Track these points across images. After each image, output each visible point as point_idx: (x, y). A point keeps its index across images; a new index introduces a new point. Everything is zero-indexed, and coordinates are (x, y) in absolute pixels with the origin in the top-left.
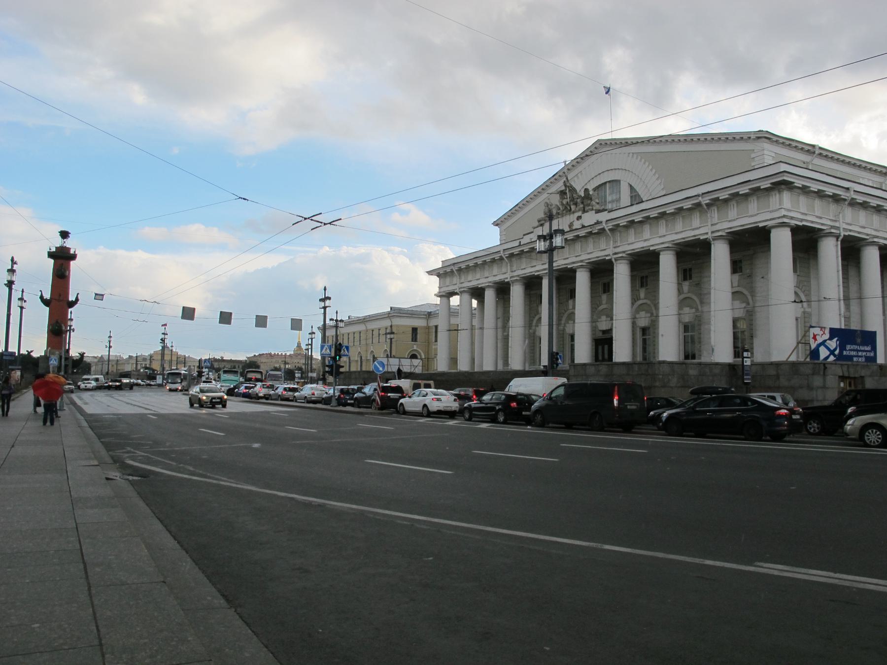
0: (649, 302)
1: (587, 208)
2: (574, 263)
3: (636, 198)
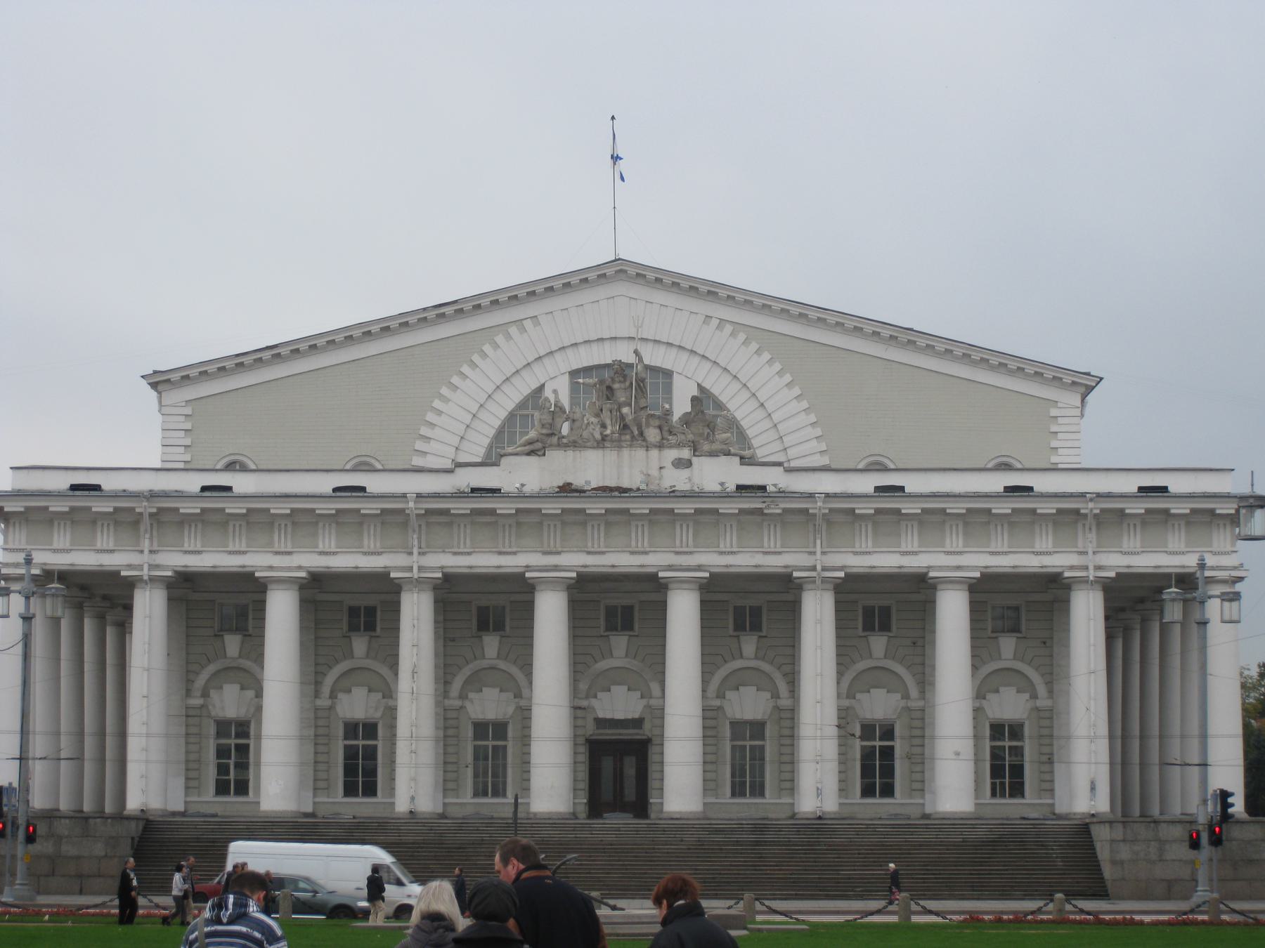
0: (765, 666)
1: (706, 447)
2: (670, 568)
3: (708, 426)
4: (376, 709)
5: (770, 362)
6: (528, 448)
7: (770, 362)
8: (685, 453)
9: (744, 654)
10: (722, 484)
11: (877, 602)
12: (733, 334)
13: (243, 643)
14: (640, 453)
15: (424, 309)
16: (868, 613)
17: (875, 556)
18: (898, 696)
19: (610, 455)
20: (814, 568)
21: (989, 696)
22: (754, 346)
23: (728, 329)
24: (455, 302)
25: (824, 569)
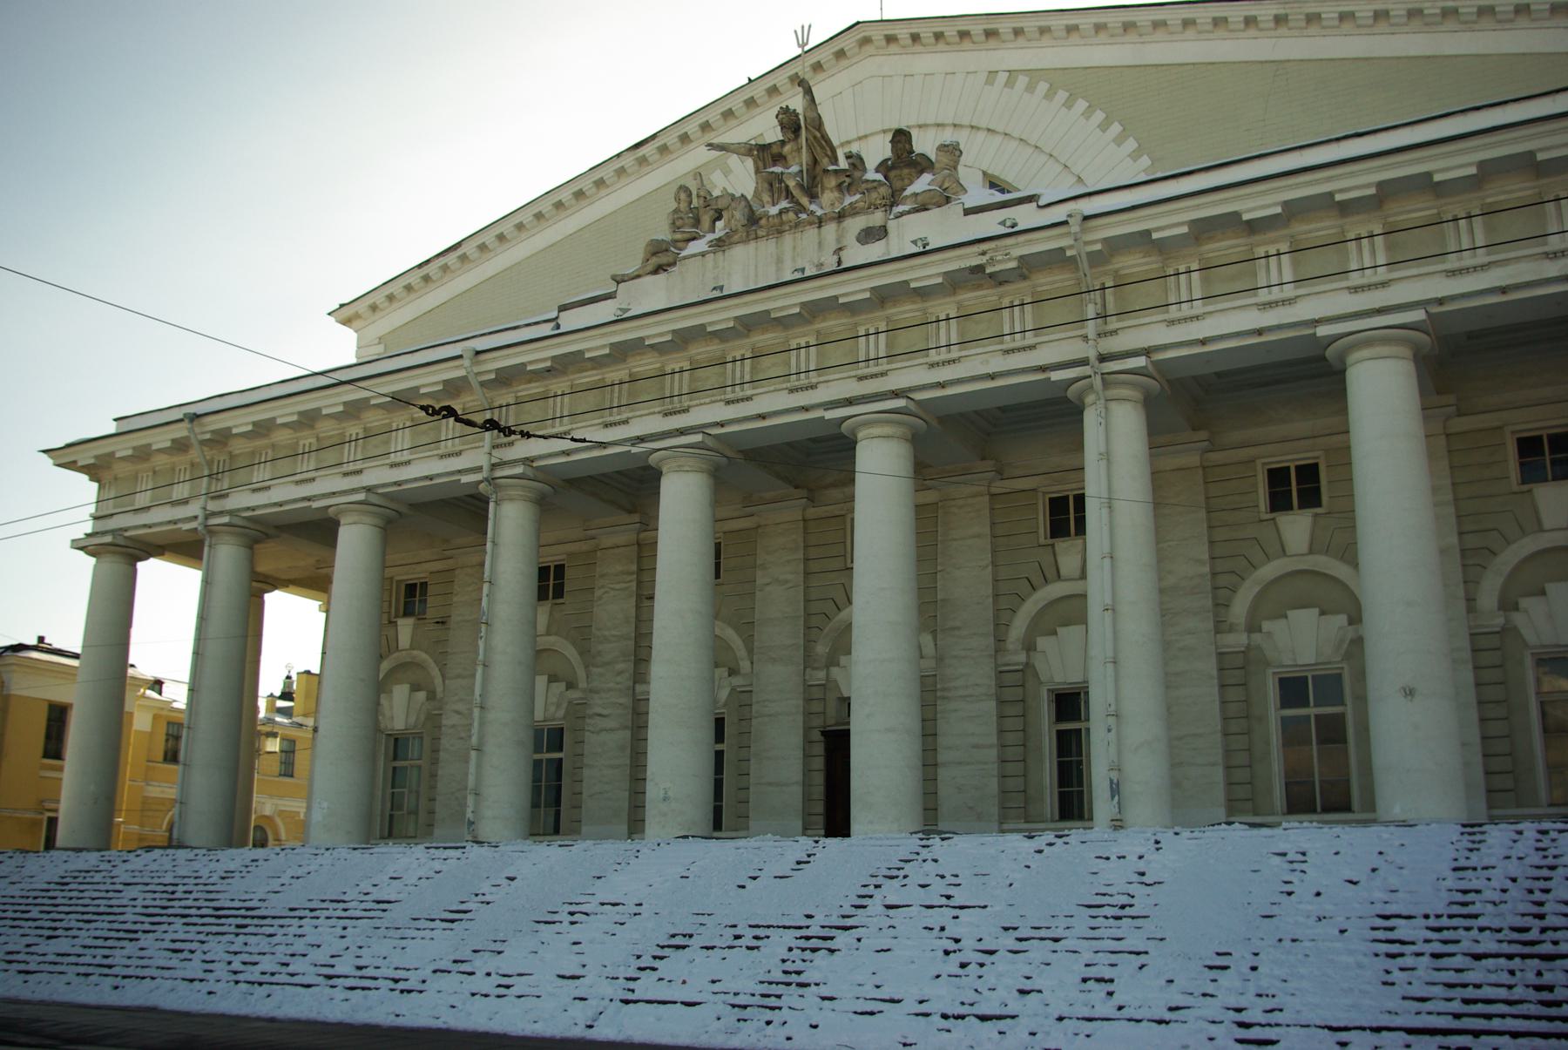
4: (558, 706)
5: (1088, 114)
6: (654, 261)
7: (1088, 114)
8: (877, 218)
9: (1063, 572)
10: (915, 242)
11: (1290, 458)
12: (1030, 88)
13: (415, 627)
14: (812, 232)
15: (618, 155)
16: (1277, 477)
17: (1209, 321)
18: (1342, 619)
19: (767, 247)
20: (1084, 362)
21: (1525, 603)
22: (1062, 95)
23: (1022, 81)
24: (654, 137)
25: (1103, 358)
